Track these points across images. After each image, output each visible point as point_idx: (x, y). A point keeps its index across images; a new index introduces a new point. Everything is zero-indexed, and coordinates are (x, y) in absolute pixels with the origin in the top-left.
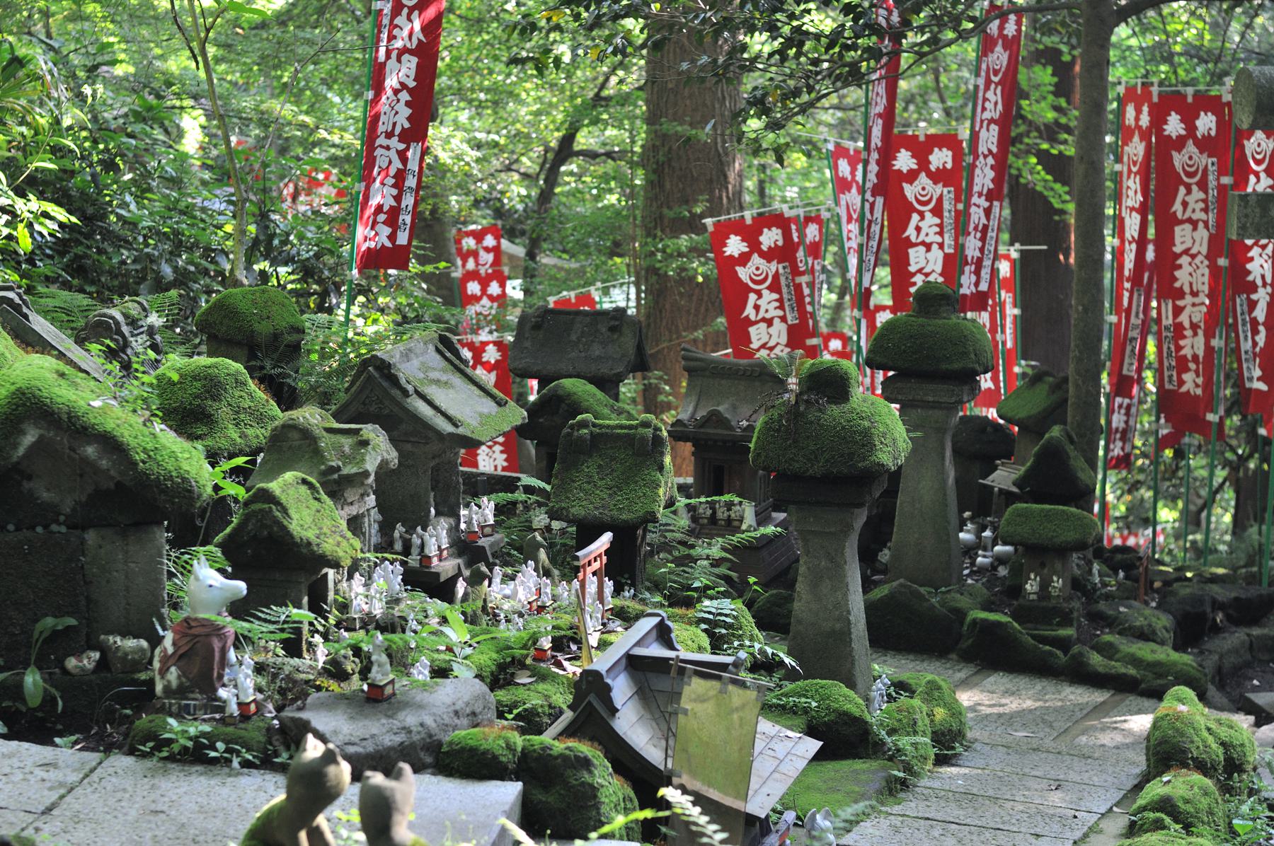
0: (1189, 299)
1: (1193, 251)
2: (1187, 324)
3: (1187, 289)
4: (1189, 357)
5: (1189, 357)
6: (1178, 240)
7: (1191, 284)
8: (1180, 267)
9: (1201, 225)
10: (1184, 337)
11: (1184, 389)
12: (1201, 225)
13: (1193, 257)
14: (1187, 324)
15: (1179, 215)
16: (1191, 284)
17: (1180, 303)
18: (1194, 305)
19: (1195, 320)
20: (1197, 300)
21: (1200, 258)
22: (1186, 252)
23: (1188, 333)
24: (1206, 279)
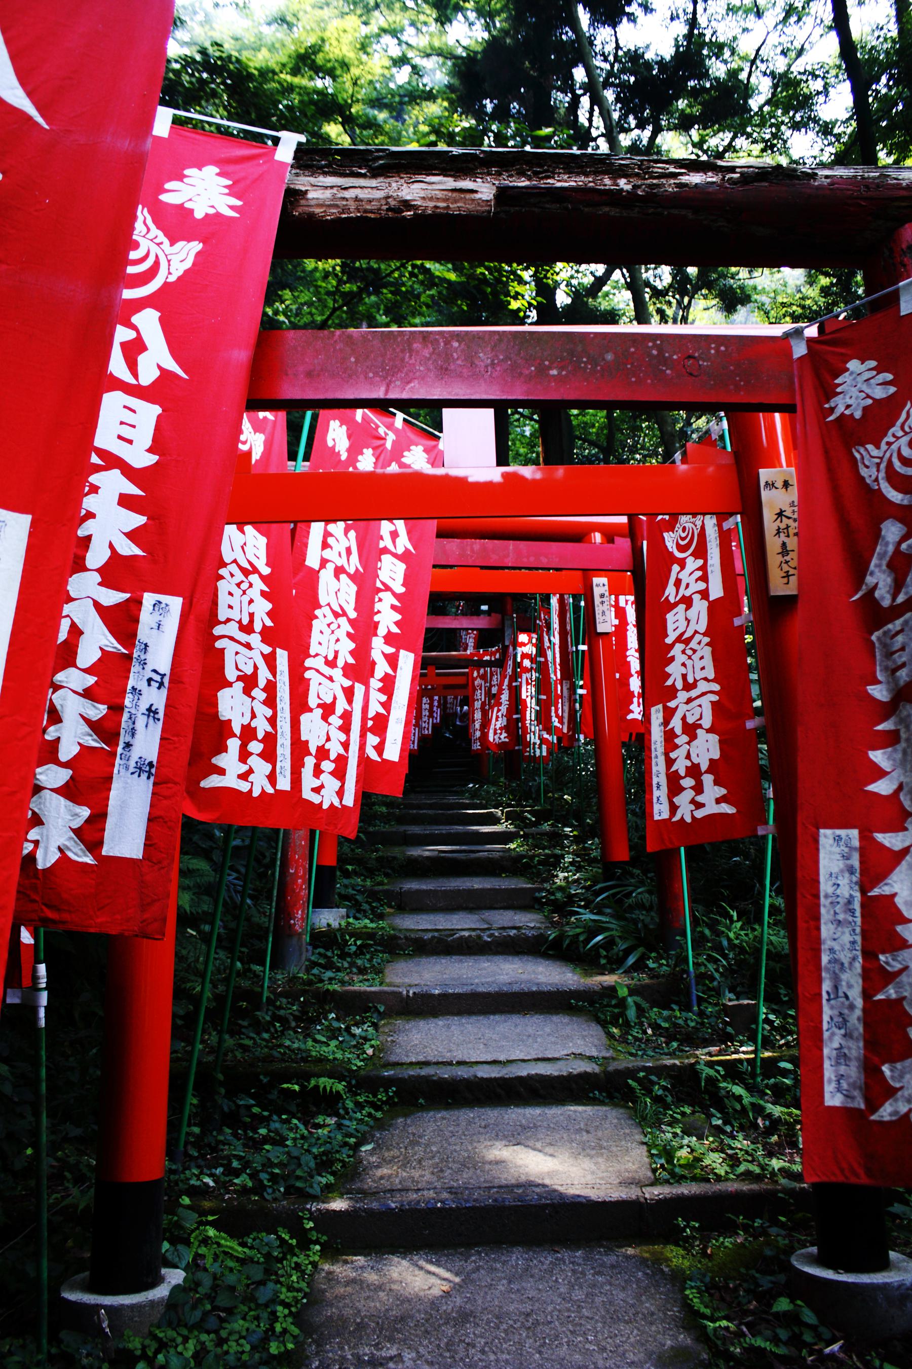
0: (682, 696)
1: (686, 636)
2: (678, 730)
3: (679, 685)
4: (682, 773)
5: (682, 773)
6: (670, 627)
7: (684, 677)
8: (673, 659)
9: (696, 598)
10: (676, 747)
11: (674, 819)
12: (696, 598)
13: (687, 641)
14: (678, 730)
15: (672, 600)
16: (684, 677)
17: (672, 704)
18: (689, 701)
19: (690, 720)
20: (694, 693)
21: (698, 637)
22: (679, 640)
23: (682, 739)
24: (708, 662)
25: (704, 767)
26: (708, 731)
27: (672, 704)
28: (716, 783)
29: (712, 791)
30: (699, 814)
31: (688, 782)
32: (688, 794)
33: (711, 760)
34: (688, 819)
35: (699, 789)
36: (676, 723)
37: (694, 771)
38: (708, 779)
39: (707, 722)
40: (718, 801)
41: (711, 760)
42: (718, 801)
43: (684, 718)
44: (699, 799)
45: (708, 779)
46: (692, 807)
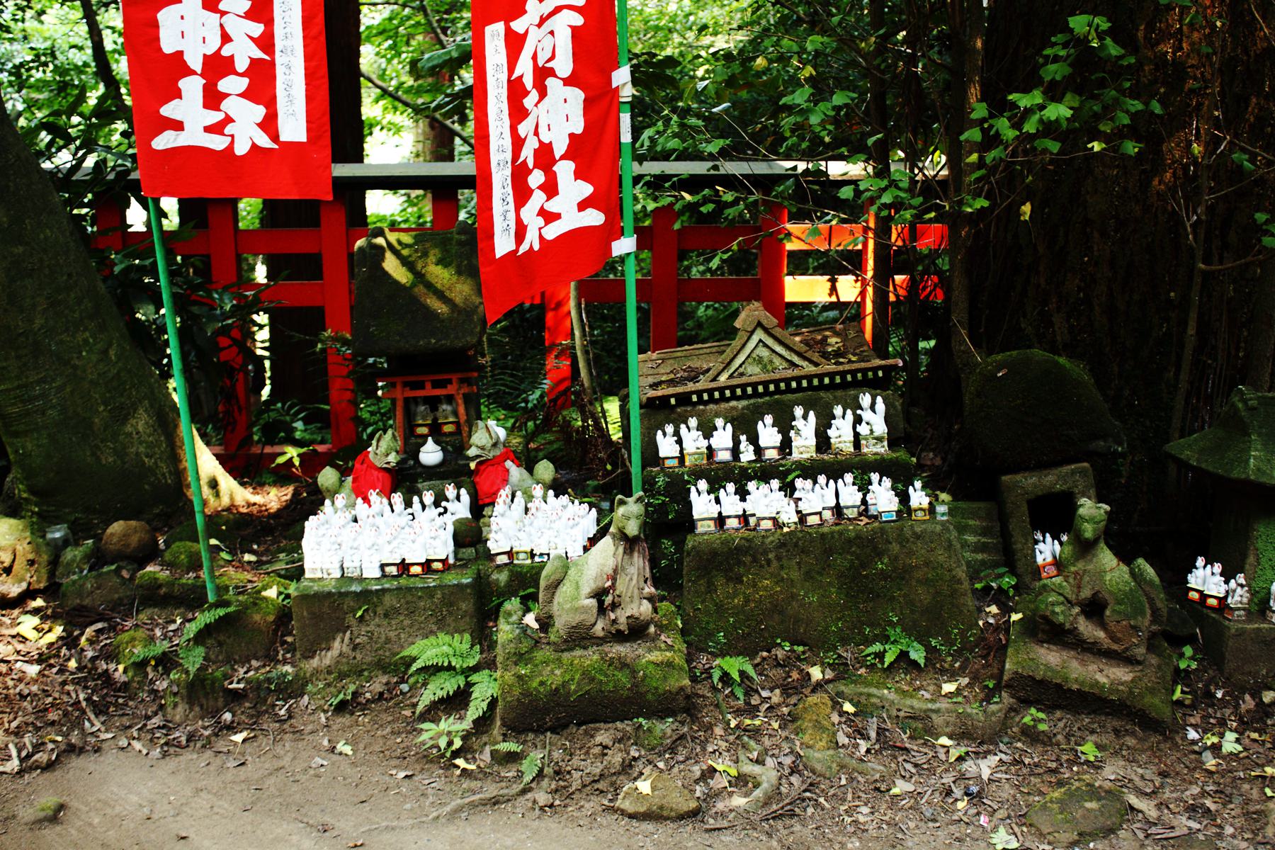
14: (528, 82)
17: (518, 26)
25: (560, 148)
26: (567, 82)
27: (518, 26)
28: (578, 175)
29: (573, 189)
30: (552, 232)
31: (536, 178)
32: (538, 198)
33: (572, 136)
34: (536, 247)
35: (551, 189)
36: (525, 68)
37: (545, 156)
38: (565, 170)
39: (564, 65)
40: (582, 206)
41: (572, 136)
42: (582, 206)
43: (535, 57)
44: (552, 206)
45: (565, 170)
46: (541, 221)
